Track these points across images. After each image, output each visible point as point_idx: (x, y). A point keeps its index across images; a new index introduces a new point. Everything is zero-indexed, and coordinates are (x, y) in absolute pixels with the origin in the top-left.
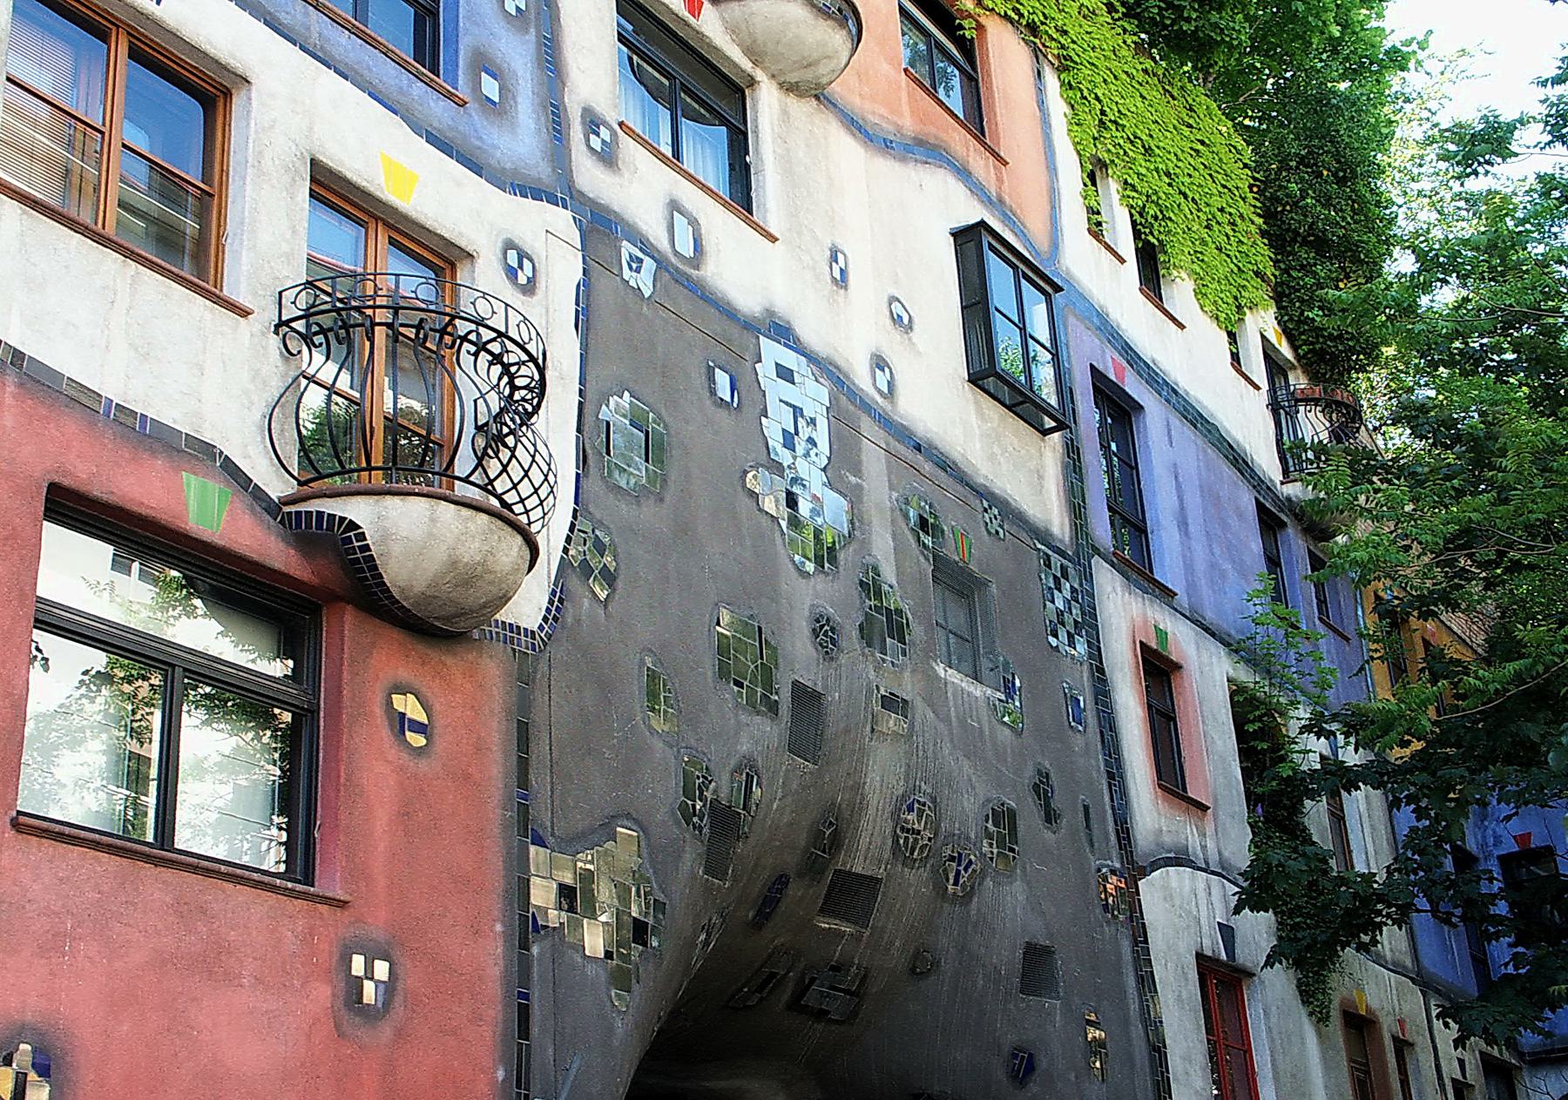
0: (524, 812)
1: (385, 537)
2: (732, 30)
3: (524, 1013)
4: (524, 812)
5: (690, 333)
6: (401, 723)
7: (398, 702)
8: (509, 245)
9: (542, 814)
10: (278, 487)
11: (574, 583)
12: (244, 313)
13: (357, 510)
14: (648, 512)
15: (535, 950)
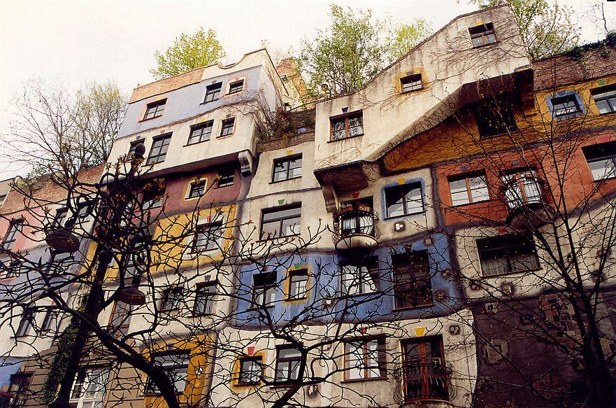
2: (516, 227)
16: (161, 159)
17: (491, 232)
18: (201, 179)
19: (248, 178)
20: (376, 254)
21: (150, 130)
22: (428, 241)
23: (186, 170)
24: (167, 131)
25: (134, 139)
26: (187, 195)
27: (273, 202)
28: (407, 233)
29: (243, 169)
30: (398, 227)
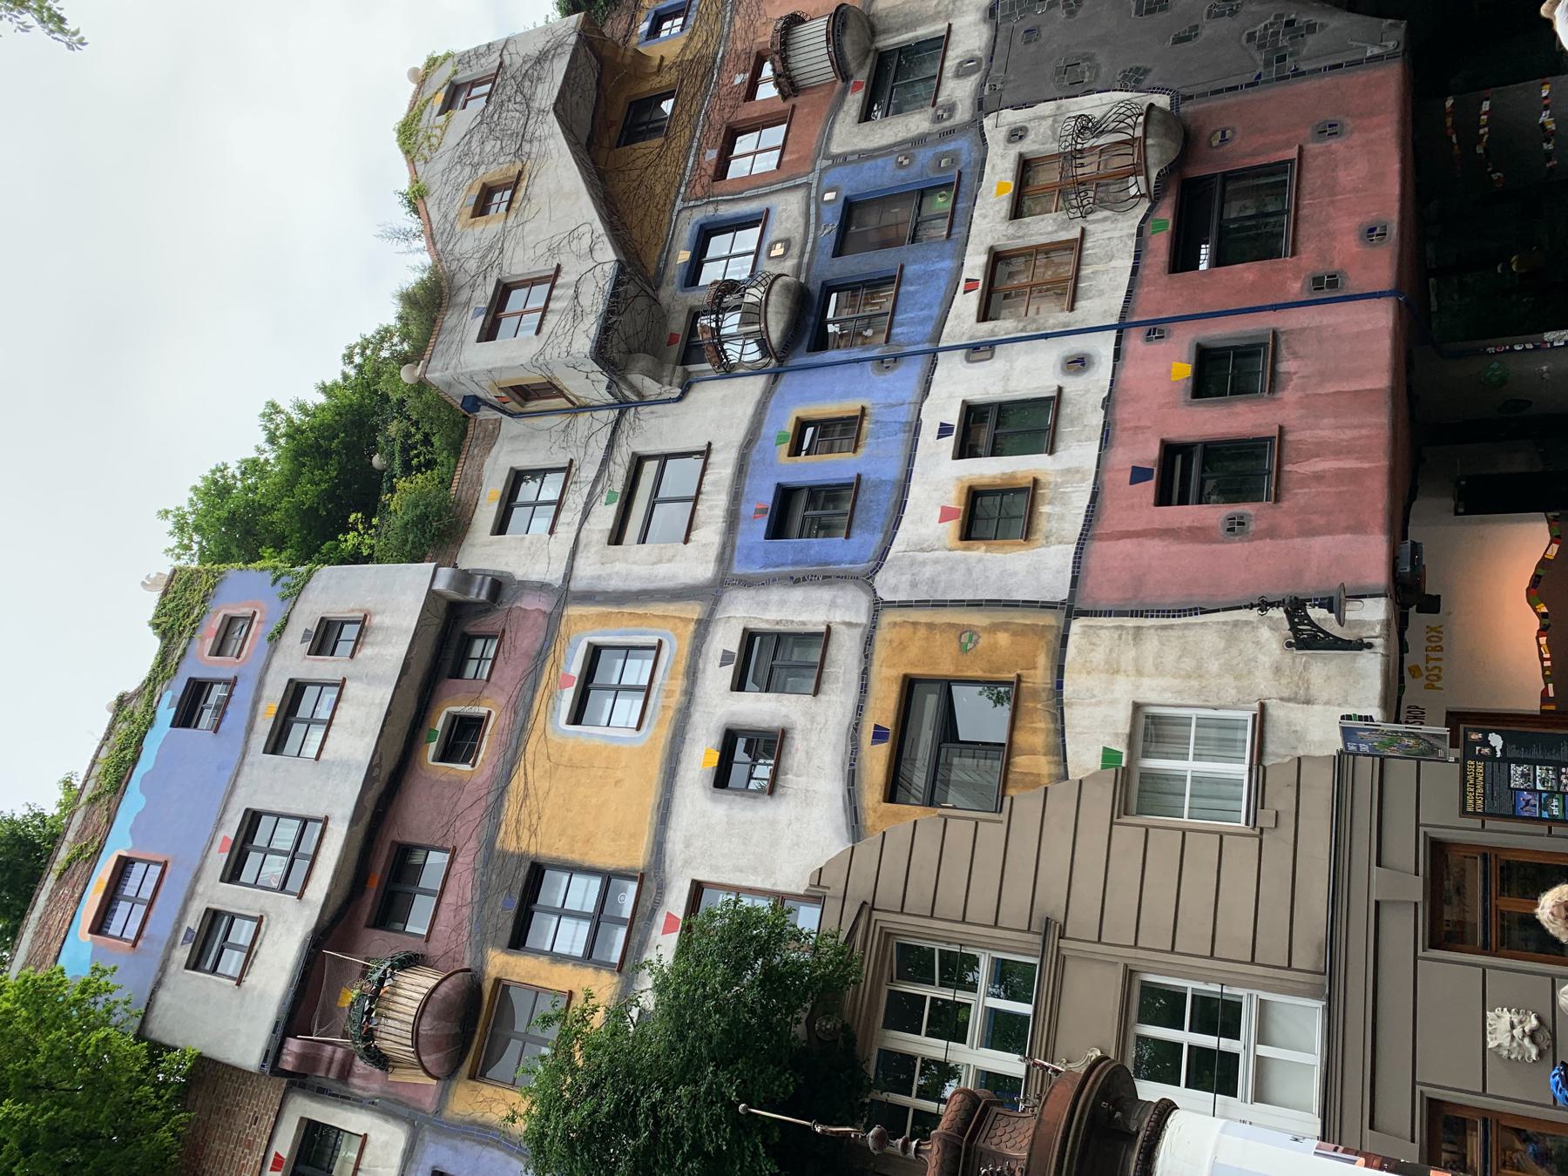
0: (1248, 85)
1: (1161, 162)
2: (861, 66)
3: (1333, 67)
4: (1248, 85)
5: (1012, 56)
6: (1224, 140)
7: (1215, 143)
8: (1009, 141)
9: (1250, 78)
10: (1146, 204)
11: (1146, 83)
12: (1083, 230)
13: (1153, 174)
14: (1101, 58)
15: (1304, 68)
16: (307, 847)
17: (854, 101)
18: (439, 727)
19: (507, 592)
20: (815, 288)
21: (190, 896)
22: (829, 196)
23: (389, 765)
24: (231, 830)
25: (182, 953)
26: (466, 767)
27: (605, 516)
28: (797, 236)
29: (478, 593)
30: (778, 250)
